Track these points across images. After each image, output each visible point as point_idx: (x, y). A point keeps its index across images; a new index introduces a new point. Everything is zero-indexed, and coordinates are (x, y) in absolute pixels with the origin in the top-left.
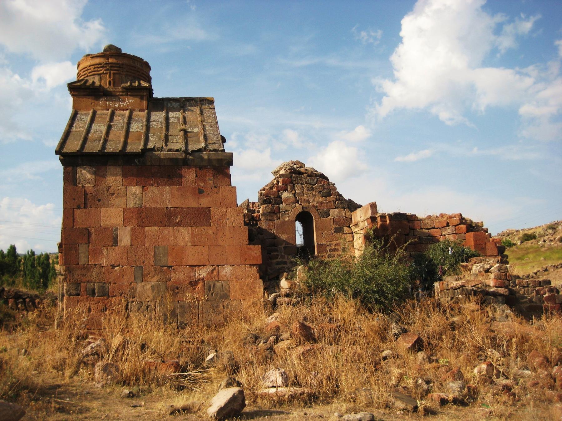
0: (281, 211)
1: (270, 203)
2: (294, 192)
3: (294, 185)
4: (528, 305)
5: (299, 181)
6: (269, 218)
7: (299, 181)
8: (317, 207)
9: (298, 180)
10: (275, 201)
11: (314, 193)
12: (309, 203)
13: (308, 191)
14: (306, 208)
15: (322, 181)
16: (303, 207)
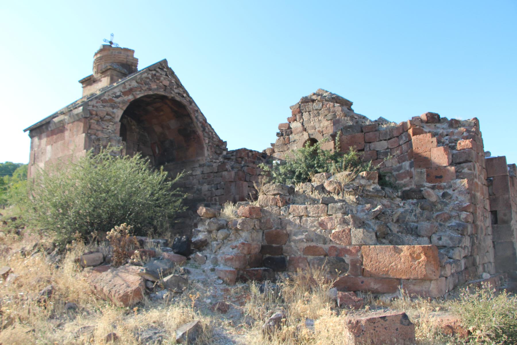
0: (290, 141)
1: (282, 135)
2: (301, 121)
3: (302, 113)
4: (305, 245)
5: (307, 109)
6: (280, 150)
7: (307, 109)
8: (322, 132)
9: (306, 108)
10: (286, 132)
11: (320, 118)
12: (315, 129)
13: (314, 117)
14: (312, 135)
15: (327, 104)
16: (309, 134)
